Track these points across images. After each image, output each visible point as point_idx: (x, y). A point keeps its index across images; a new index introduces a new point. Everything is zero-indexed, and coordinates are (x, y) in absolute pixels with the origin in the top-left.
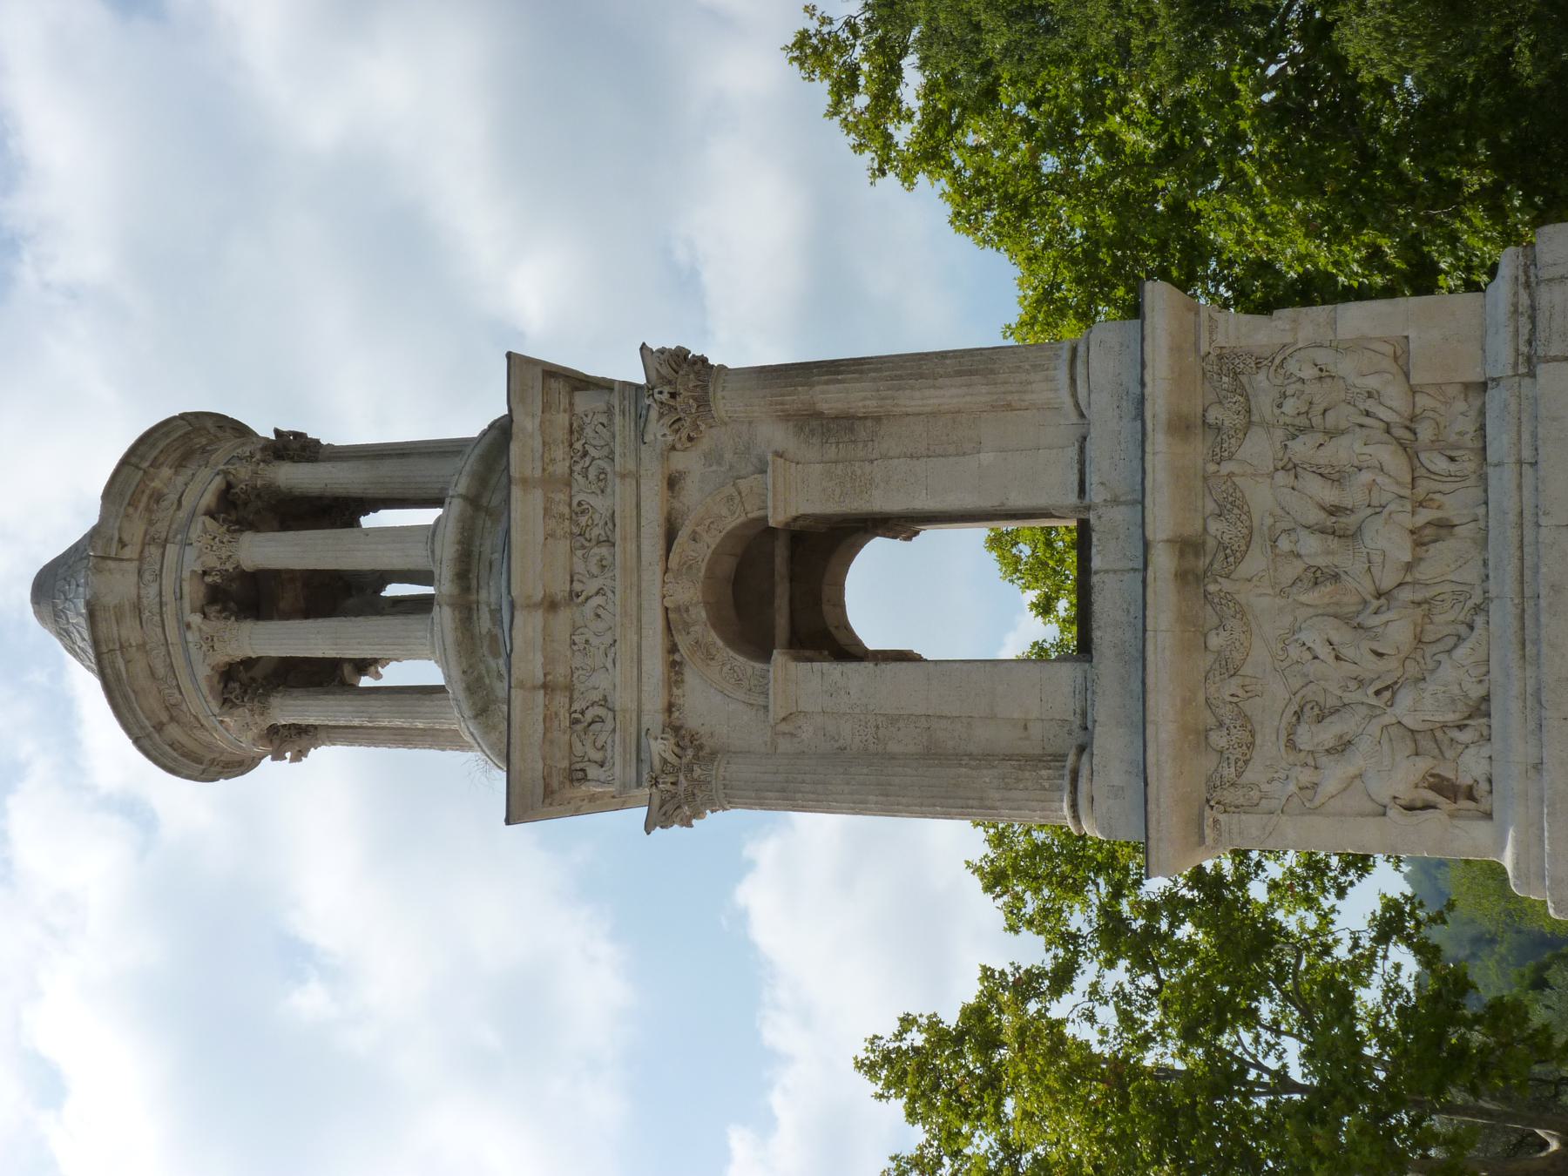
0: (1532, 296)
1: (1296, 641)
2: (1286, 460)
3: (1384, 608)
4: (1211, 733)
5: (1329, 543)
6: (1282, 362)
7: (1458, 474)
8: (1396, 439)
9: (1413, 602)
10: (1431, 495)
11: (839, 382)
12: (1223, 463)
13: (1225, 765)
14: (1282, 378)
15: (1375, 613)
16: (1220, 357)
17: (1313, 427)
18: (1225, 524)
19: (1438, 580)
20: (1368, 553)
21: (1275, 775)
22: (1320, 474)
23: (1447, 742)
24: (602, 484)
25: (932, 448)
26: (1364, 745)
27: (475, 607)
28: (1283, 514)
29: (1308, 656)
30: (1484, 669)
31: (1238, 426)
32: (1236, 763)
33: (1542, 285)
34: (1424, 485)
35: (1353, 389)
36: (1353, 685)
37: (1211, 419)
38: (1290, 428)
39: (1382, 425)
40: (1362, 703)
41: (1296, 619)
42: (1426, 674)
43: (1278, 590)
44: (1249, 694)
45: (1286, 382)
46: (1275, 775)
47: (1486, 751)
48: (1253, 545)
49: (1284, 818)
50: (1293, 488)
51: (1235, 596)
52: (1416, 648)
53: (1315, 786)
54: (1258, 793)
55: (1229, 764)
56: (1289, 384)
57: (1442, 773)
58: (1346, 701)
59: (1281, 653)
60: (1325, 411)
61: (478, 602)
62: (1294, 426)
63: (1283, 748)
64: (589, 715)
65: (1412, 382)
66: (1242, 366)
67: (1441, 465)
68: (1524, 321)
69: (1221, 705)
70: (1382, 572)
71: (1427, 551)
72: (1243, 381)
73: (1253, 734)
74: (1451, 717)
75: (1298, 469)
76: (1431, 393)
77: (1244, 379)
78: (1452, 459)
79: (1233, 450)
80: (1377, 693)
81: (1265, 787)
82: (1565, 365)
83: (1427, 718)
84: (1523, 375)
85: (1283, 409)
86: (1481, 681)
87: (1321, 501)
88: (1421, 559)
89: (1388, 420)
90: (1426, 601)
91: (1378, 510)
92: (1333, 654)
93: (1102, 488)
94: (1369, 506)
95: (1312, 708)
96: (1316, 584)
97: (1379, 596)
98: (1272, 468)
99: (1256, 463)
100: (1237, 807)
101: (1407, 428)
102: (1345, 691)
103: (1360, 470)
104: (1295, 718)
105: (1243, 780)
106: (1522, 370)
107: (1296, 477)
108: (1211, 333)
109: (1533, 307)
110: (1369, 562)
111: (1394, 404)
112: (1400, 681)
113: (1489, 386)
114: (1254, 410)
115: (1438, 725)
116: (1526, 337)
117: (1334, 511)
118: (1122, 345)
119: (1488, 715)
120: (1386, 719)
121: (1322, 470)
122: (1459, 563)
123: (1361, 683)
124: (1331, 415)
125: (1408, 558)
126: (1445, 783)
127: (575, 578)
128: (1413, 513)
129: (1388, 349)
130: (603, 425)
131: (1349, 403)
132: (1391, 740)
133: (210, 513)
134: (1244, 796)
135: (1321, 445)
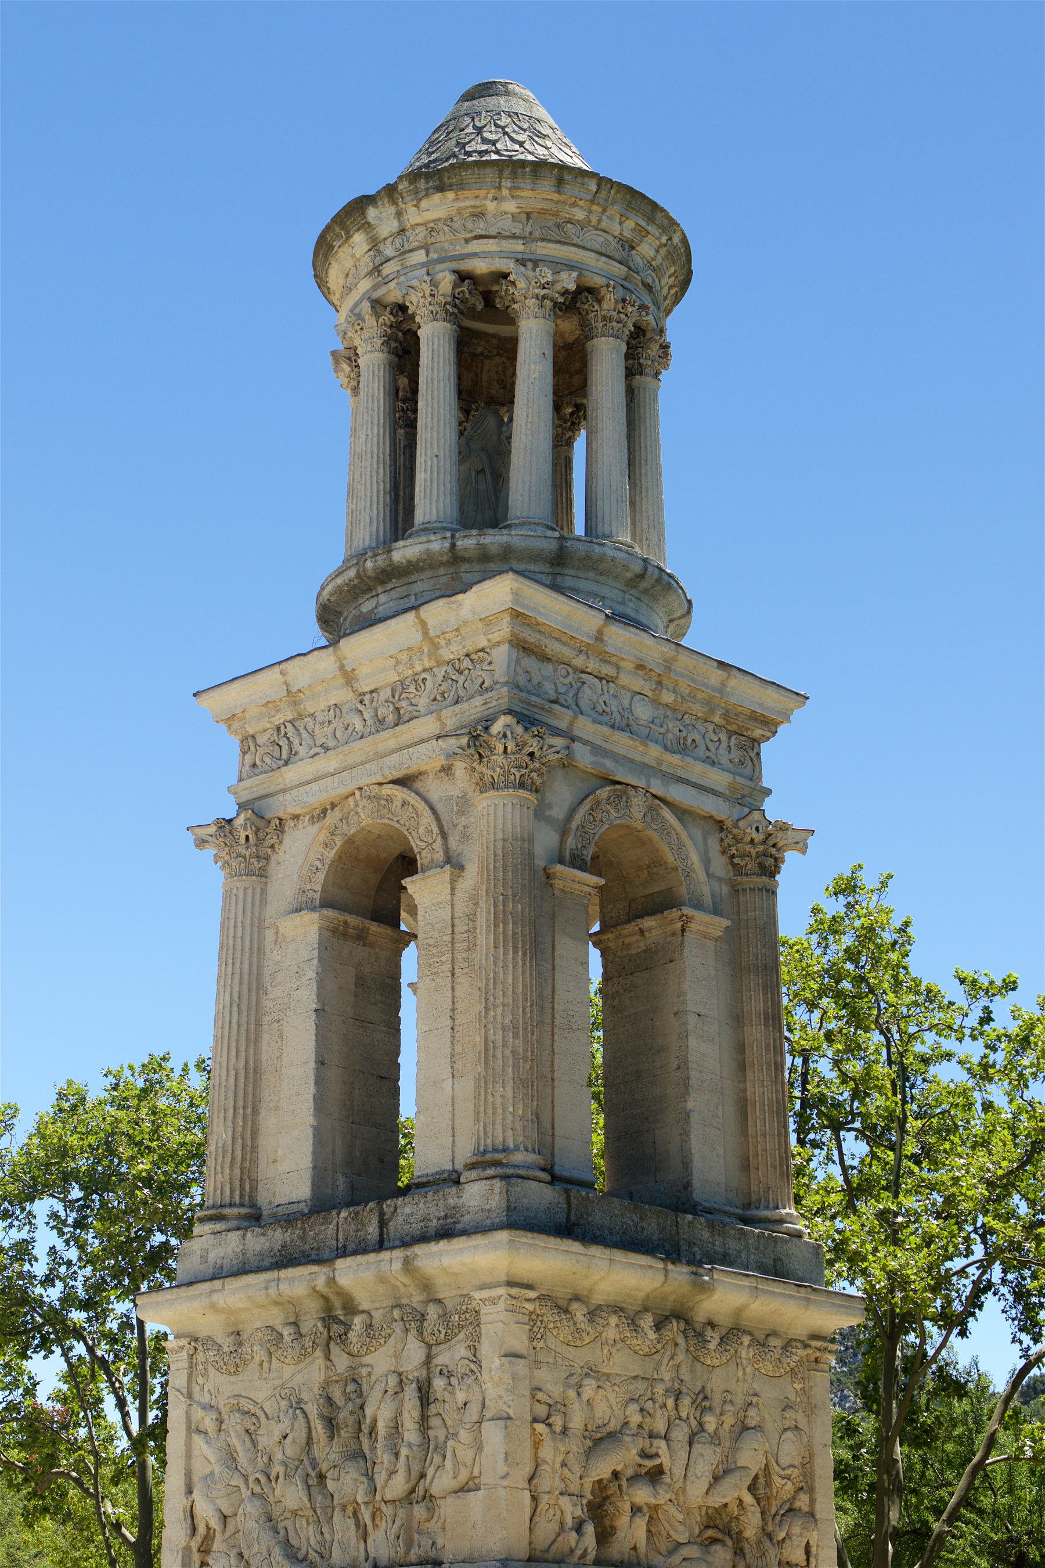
11: (488, 926)
24: (439, 698)
25: (460, 1029)
27: (374, 593)
61: (378, 595)
64: (283, 743)
80: (258, 1480)
93: (392, 1209)
98: (401, 1370)
118: (489, 1211)
127: (374, 695)
129: (476, 1473)
130: (483, 683)
133: (462, 277)
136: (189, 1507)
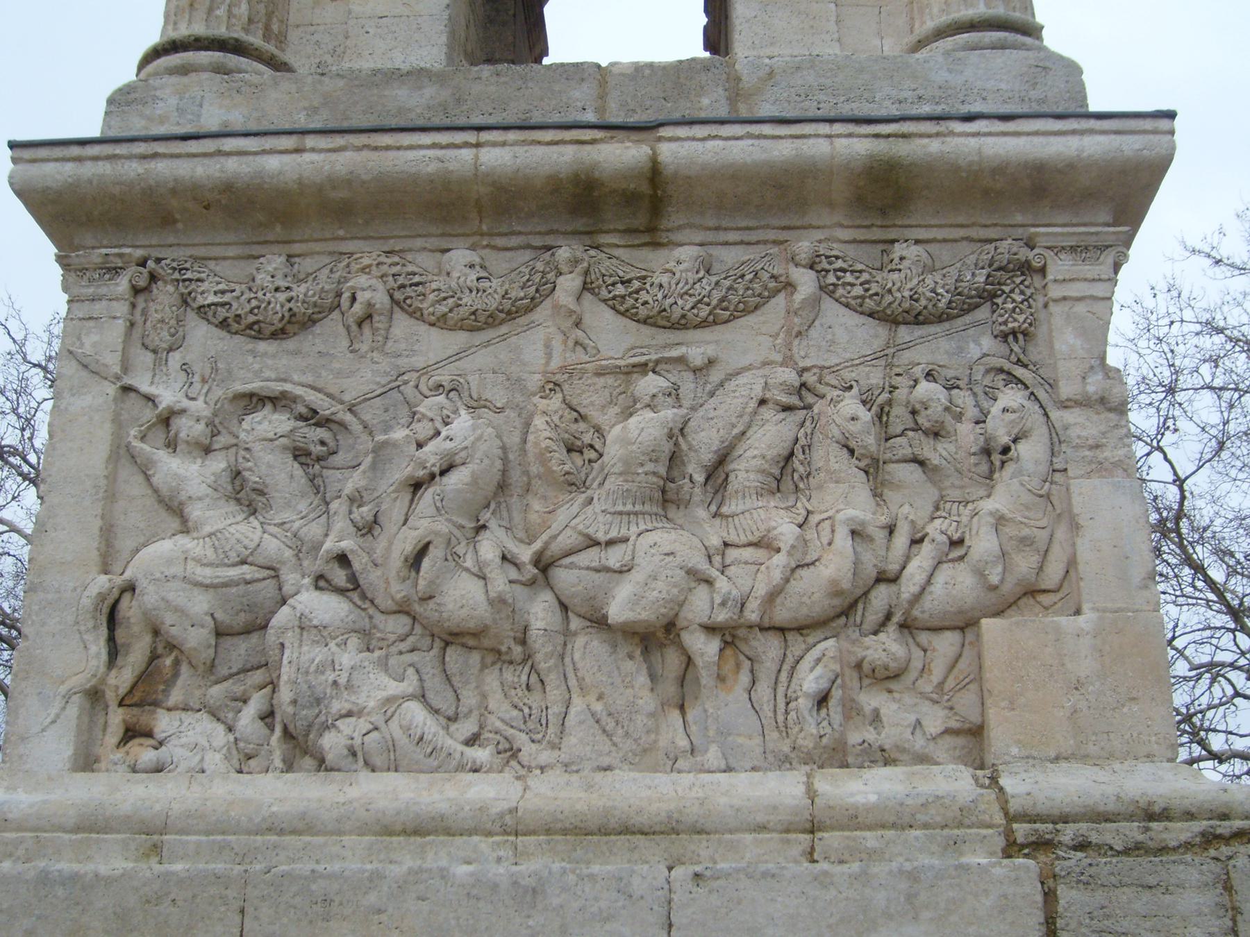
0: (1187, 846)
1: (456, 412)
2: (822, 389)
3: (513, 574)
4: (283, 259)
5: (650, 467)
6: (1019, 381)
7: (793, 715)
8: (866, 594)
9: (526, 629)
10: (748, 663)
12: (812, 274)
13: (222, 287)
14: (987, 381)
15: (504, 558)
16: (1025, 268)
17: (887, 440)
18: (692, 277)
19: (573, 682)
20: (626, 540)
21: (197, 378)
22: (792, 454)
23: (238, 689)
26: (245, 532)
28: (709, 387)
29: (423, 429)
30: (378, 761)
31: (889, 298)
32: (223, 305)
33: (1217, 868)
34: (769, 648)
36: (366, 511)
37: (898, 250)
38: (885, 396)
39: (893, 567)
40: (327, 535)
41: (500, 410)
42: (377, 653)
43: (559, 378)
44: (354, 328)
45: (978, 389)
46: (197, 378)
47: (214, 760)
48: (646, 330)
49: (111, 390)
50: (763, 402)
51: (548, 303)
52: (433, 635)
53: (172, 445)
54: (164, 345)
55: (223, 292)
56: (975, 395)
57: (180, 682)
58: (334, 506)
59: (431, 382)
60: (921, 463)
62: (890, 402)
63: (249, 387)
65: (984, 621)
66: (1010, 306)
67: (810, 680)
68: (1132, 831)
69: (337, 275)
70: (588, 568)
71: (631, 657)
72: (982, 308)
73: (279, 334)
74: (285, 694)
75: (805, 412)
76: (962, 665)
77: (983, 313)
78: (822, 700)
79: (840, 291)
81: (175, 359)
82: (1037, 917)
83: (287, 653)
84: (1009, 833)
85: (925, 387)
86: (354, 754)
87: (736, 454)
88: (614, 646)
89: (903, 579)
90: (527, 657)
91: (717, 559)
92: (421, 473)
94: (726, 544)
95: (323, 443)
96: (569, 451)
97: (544, 565)
98: (802, 364)
99: (813, 333)
100: (144, 313)
101: (888, 617)
102: (352, 500)
103: (800, 526)
104: (303, 410)
105: (191, 316)
106: (1021, 831)
107: (787, 408)
108: (1073, 249)
109: (1163, 850)
110: (610, 543)
111: (938, 587)
112: (367, 605)
113: (980, 773)
115: (274, 676)
116: (1094, 838)
117: (718, 470)
119: (289, 767)
120: (290, 578)
121: (801, 457)
122: (605, 719)
123: (369, 528)
124: (910, 473)
125: (617, 611)
126: (162, 687)
128: (710, 629)
131: (937, 508)
132: (248, 583)
134: (162, 321)
135: (852, 452)
136: (110, 601)
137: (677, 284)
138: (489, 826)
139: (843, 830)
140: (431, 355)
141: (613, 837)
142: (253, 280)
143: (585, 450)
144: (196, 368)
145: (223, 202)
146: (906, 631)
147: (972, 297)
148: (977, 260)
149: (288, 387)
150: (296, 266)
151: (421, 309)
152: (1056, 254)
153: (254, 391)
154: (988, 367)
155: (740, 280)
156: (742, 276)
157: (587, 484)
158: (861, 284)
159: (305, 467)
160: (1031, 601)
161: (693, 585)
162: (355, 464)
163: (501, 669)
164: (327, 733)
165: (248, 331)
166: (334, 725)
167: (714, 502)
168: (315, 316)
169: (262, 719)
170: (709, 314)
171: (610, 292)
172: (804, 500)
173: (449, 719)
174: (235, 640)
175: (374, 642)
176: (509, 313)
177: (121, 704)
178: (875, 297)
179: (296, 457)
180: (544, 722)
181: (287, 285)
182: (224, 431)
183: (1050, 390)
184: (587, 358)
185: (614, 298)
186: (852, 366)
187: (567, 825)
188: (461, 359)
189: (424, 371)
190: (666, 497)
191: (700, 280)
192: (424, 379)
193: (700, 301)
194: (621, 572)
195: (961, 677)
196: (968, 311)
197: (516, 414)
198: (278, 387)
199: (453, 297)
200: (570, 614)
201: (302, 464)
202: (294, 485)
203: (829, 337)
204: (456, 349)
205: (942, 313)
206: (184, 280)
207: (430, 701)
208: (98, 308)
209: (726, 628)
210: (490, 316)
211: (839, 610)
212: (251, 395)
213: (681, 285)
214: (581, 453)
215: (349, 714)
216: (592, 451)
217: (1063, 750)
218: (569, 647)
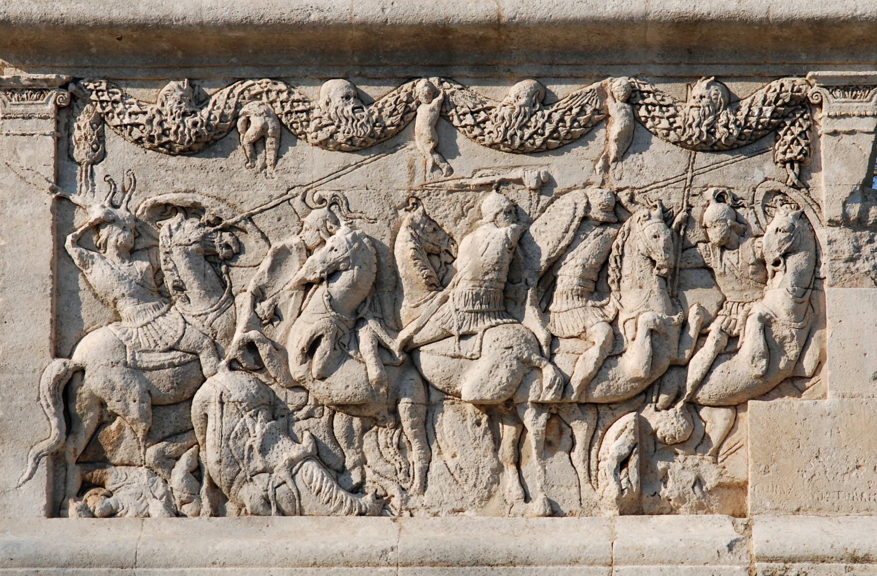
17: (683, 250)
28: (541, 204)
31: (689, 132)
35: (742, 312)
42: (281, 421)
59: (316, 197)
66: (789, 138)
96: (429, 254)
114: (714, 158)
137: (517, 117)
138: (377, 560)
139: (634, 564)
140: (315, 172)
141: (468, 568)
142: (163, 105)
143: (442, 255)
144: (118, 180)
145: (135, 36)
146: (692, 406)
147: (759, 130)
148: (765, 96)
149: (198, 198)
150: (196, 88)
151: (305, 133)
152: (831, 93)
153: (170, 202)
154: (768, 189)
155: (568, 113)
156: (571, 109)
157: (444, 283)
158: (668, 118)
159: (214, 265)
160: (790, 385)
161: (528, 371)
162: (256, 263)
163: (377, 432)
164: (246, 484)
165: (161, 149)
166: (251, 480)
167: (544, 300)
168: (216, 137)
169: (191, 472)
170: (543, 144)
171: (461, 121)
172: (615, 301)
173: (337, 471)
174: (166, 410)
175: (278, 412)
176: (379, 138)
177: (77, 463)
178: (678, 130)
179: (206, 257)
180: (411, 475)
181: (191, 109)
182: (144, 234)
183: (817, 211)
184: (442, 178)
185: (465, 126)
186: (657, 188)
187: (435, 559)
188: (339, 177)
189: (308, 187)
190: (508, 296)
191: (535, 113)
192: (309, 193)
193: (536, 133)
194: (472, 359)
195: (733, 444)
196: (756, 140)
197: (386, 225)
198: (189, 199)
199: (333, 124)
200: (430, 388)
201: (210, 263)
202: (207, 282)
203: (639, 163)
204: (336, 167)
205: (734, 144)
206: (102, 102)
207: (323, 458)
208: (28, 126)
209: (552, 404)
210: (364, 141)
211: (639, 391)
212: (167, 205)
213: (520, 118)
214: (438, 255)
215: (264, 471)
216: (448, 255)
217: (803, 504)
218: (430, 415)
